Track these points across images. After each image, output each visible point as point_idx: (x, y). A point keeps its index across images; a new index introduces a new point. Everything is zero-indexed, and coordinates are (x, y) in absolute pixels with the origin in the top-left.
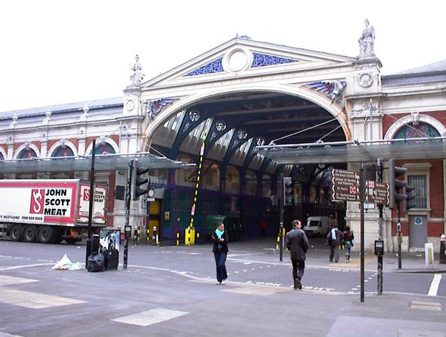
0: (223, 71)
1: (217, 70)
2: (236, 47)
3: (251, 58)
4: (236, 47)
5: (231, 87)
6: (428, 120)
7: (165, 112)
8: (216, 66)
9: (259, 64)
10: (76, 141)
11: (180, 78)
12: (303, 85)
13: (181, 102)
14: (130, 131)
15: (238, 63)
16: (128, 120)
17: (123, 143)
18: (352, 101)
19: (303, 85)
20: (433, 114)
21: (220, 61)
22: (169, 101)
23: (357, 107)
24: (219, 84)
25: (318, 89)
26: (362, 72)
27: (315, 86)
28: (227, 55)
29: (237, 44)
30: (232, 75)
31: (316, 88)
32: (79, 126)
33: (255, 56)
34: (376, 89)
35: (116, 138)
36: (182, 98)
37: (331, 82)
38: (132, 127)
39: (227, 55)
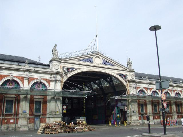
4: (98, 56)
5: (96, 69)
6: (144, 89)
7: (71, 74)
8: (90, 60)
10: (22, 79)
11: (77, 61)
14: (57, 79)
15: (98, 61)
16: (57, 73)
17: (52, 84)
18: (130, 81)
20: (145, 88)
21: (91, 58)
22: (74, 69)
23: (131, 83)
24: (92, 67)
26: (132, 74)
27: (120, 75)
29: (98, 55)
30: (96, 65)
32: (24, 71)
34: (134, 79)
35: (49, 81)
36: (78, 69)
37: (126, 75)
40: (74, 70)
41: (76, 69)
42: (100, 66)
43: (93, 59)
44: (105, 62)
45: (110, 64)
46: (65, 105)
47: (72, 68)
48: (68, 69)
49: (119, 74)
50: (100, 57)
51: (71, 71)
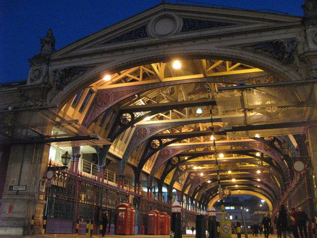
0: (147, 36)
2: (163, 13)
3: (180, 24)
21: (144, 27)
29: (165, 10)
33: (185, 21)
42: (173, 37)
50: (173, 14)
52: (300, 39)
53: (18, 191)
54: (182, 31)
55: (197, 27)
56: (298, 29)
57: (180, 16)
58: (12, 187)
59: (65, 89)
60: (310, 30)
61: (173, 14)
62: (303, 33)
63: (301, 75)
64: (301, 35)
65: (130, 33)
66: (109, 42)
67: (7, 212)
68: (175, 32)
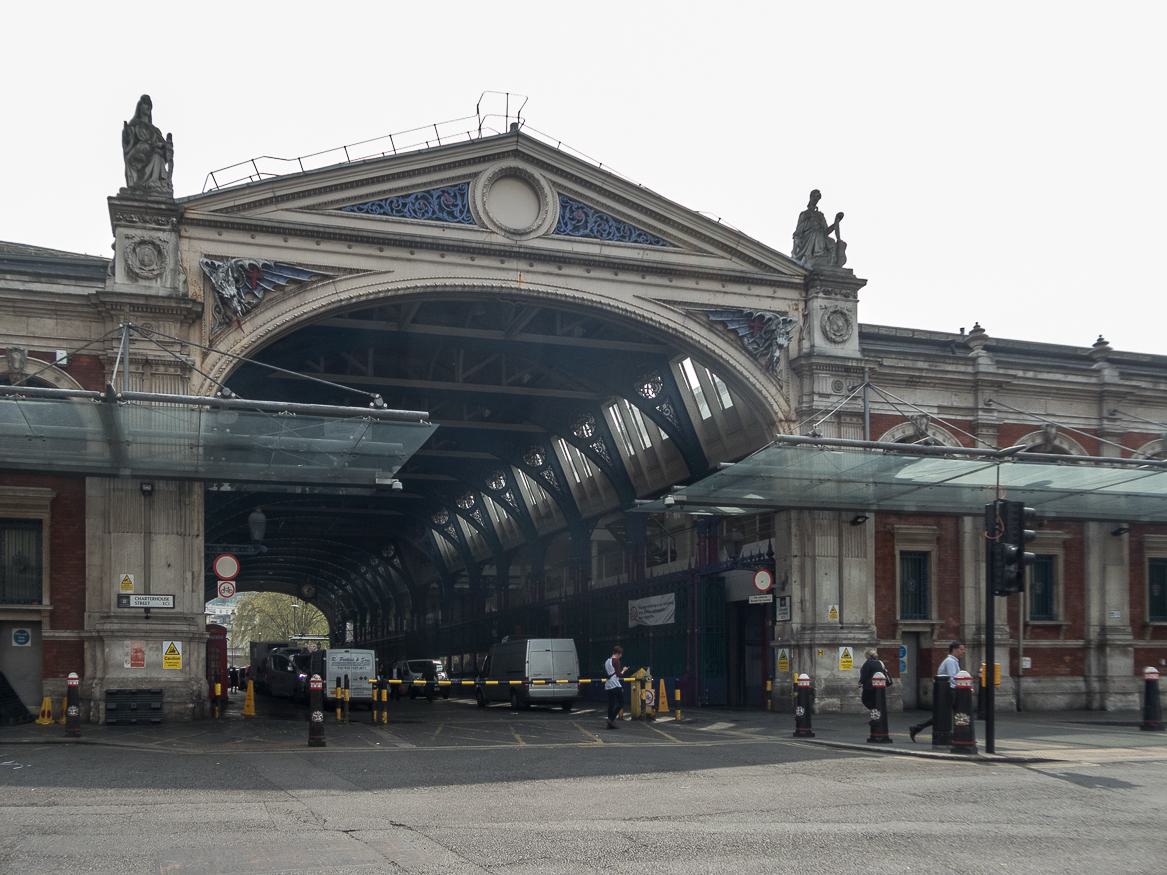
1: (451, 214)
8: (451, 203)
9: (576, 228)
12: (691, 311)
13: (342, 286)
18: (804, 367)
19: (691, 311)
21: (461, 191)
22: (301, 278)
25: (731, 327)
28: (483, 180)
29: (516, 154)
30: (499, 239)
31: (724, 323)
37: (768, 315)
38: (155, 337)
39: (488, 174)
40: (302, 286)
41: (325, 275)
42: (534, 243)
43: (477, 193)
44: (574, 217)
45: (624, 232)
46: (237, 558)
47: (279, 266)
48: (251, 276)
49: (707, 314)
50: (536, 172)
51: (277, 287)
52: (796, 316)
53: (147, 610)
54: (558, 231)
55: (592, 230)
56: (794, 294)
57: (554, 183)
58: (127, 597)
59: (247, 327)
60: (819, 303)
61: (536, 172)
62: (801, 306)
63: (787, 401)
64: (797, 309)
65: (426, 197)
66: (361, 207)
67: (129, 666)
68: (541, 232)
